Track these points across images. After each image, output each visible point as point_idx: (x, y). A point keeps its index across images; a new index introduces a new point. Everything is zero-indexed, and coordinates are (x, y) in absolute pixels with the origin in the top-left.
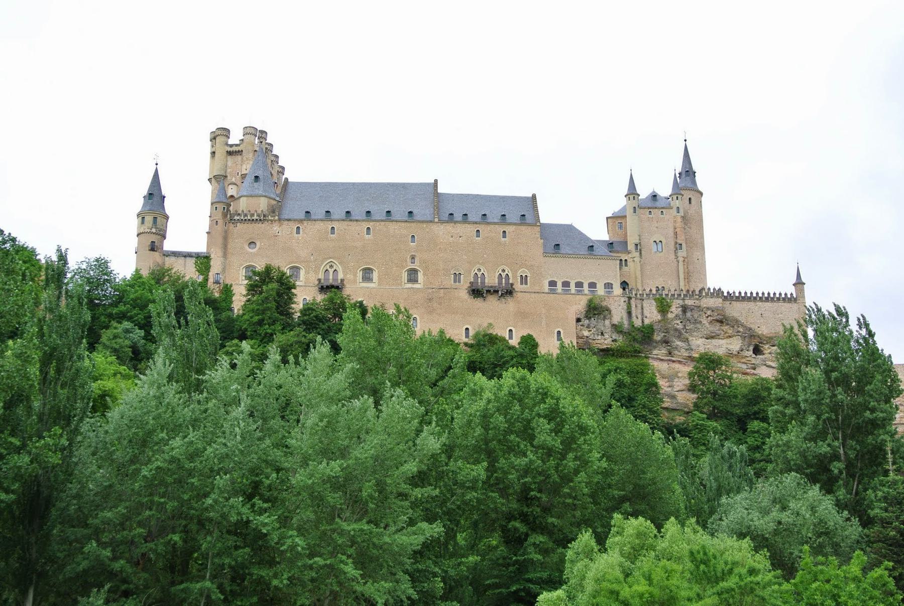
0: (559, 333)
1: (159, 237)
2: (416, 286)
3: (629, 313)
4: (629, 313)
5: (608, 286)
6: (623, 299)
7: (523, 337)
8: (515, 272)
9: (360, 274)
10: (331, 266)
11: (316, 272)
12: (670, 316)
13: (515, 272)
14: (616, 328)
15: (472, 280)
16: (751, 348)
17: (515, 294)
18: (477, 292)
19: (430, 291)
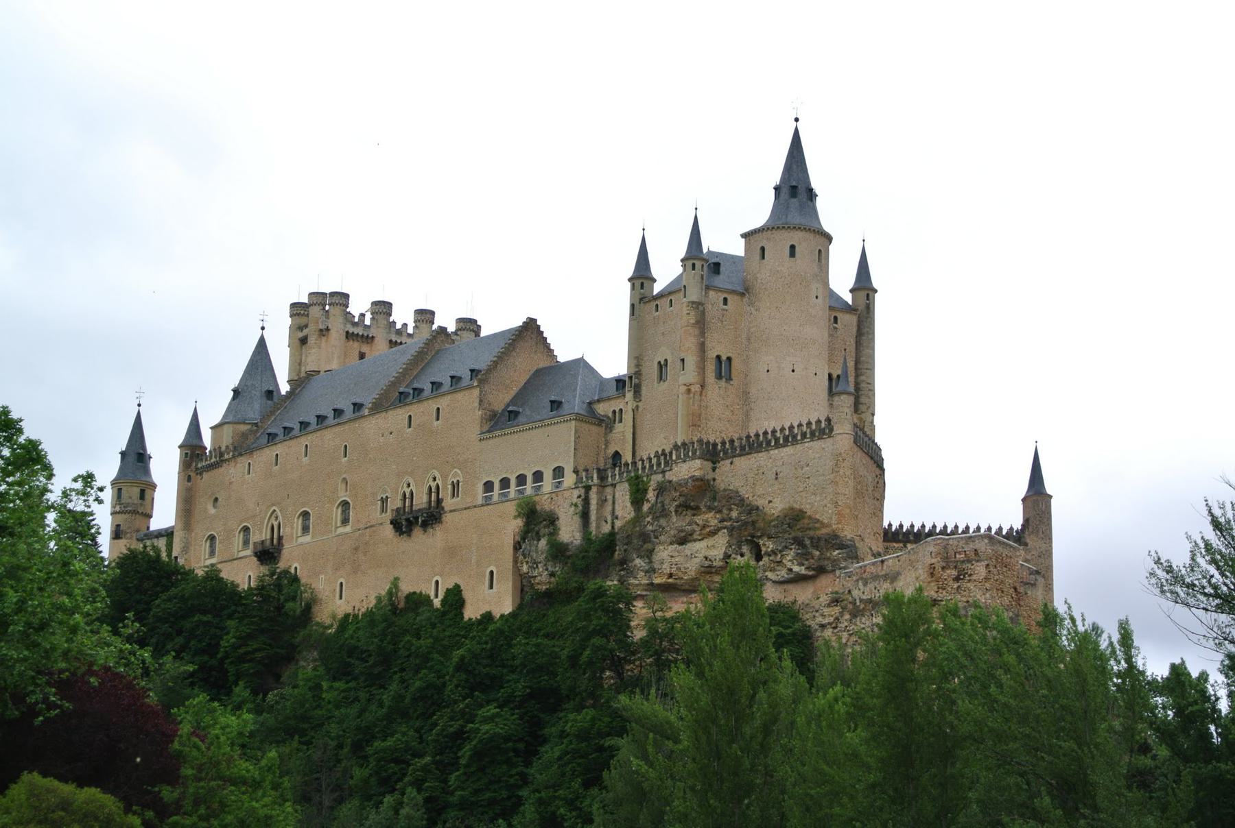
0: (492, 572)
1: (126, 516)
2: (348, 529)
3: (585, 515)
4: (585, 515)
5: (558, 472)
6: (576, 493)
8: (445, 477)
11: (261, 532)
12: (646, 507)
13: (445, 477)
14: (558, 552)
15: (399, 504)
16: (745, 549)
17: (444, 519)
18: (406, 523)
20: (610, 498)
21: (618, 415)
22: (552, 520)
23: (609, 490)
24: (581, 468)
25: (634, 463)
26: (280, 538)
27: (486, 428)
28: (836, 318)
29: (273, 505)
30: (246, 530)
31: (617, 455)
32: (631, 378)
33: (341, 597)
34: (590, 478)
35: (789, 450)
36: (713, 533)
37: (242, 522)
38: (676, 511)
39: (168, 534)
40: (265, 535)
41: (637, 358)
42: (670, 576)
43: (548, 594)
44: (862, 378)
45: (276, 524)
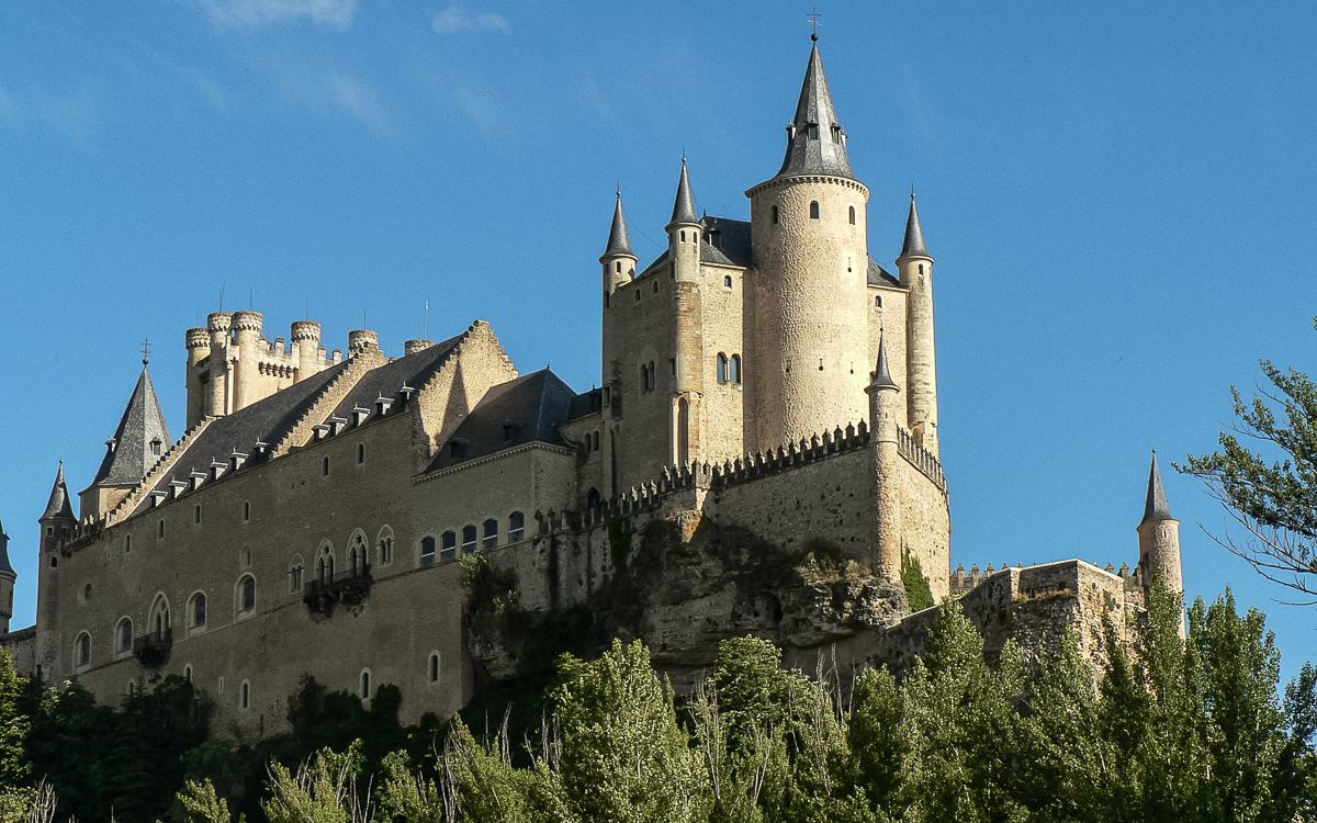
0: (435, 658)
2: (253, 613)
4: (552, 573)
5: (517, 519)
7: (381, 687)
8: (371, 536)
9: (191, 609)
10: (164, 605)
11: (144, 625)
13: (371, 536)
14: (517, 623)
15: (316, 576)
16: (760, 605)
19: (264, 617)
20: (584, 549)
21: (594, 441)
22: (510, 581)
23: (583, 538)
24: (545, 513)
25: (614, 501)
26: (169, 632)
27: (422, 468)
28: (878, 298)
29: (158, 589)
30: (127, 624)
31: (594, 494)
32: (607, 389)
33: (245, 705)
34: (556, 524)
35: (811, 470)
36: (717, 588)
37: (120, 615)
38: (668, 560)
39: (28, 635)
40: (151, 628)
41: (615, 363)
42: (664, 647)
43: (508, 682)
44: (917, 377)
45: (163, 613)
